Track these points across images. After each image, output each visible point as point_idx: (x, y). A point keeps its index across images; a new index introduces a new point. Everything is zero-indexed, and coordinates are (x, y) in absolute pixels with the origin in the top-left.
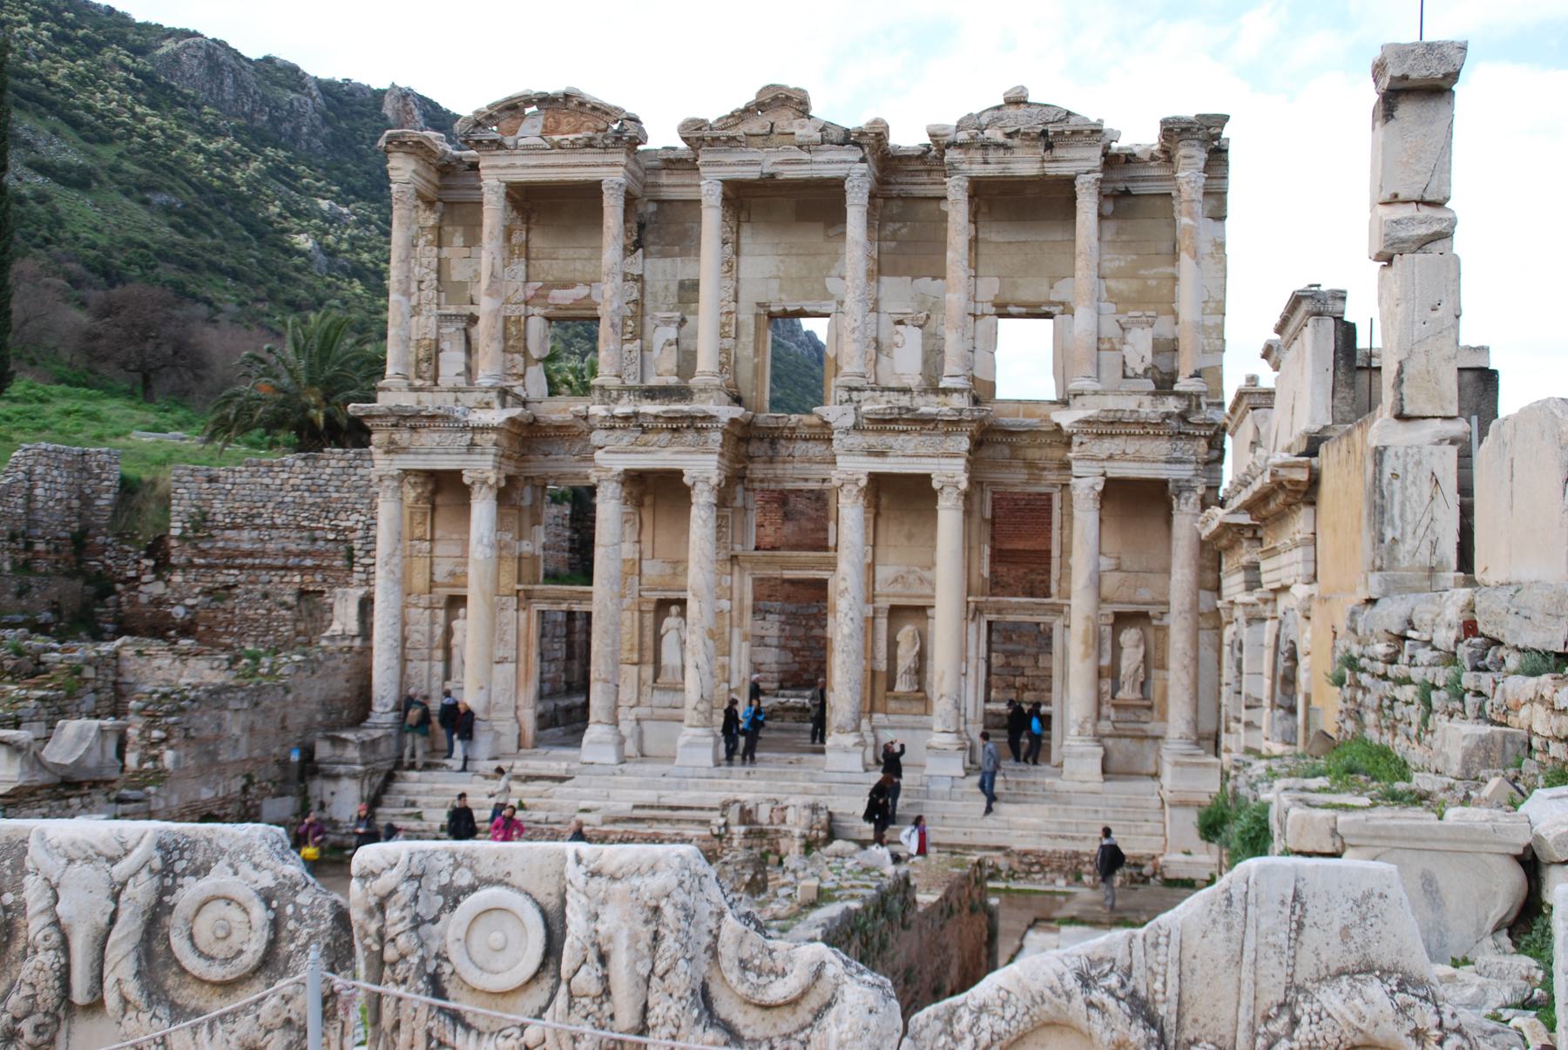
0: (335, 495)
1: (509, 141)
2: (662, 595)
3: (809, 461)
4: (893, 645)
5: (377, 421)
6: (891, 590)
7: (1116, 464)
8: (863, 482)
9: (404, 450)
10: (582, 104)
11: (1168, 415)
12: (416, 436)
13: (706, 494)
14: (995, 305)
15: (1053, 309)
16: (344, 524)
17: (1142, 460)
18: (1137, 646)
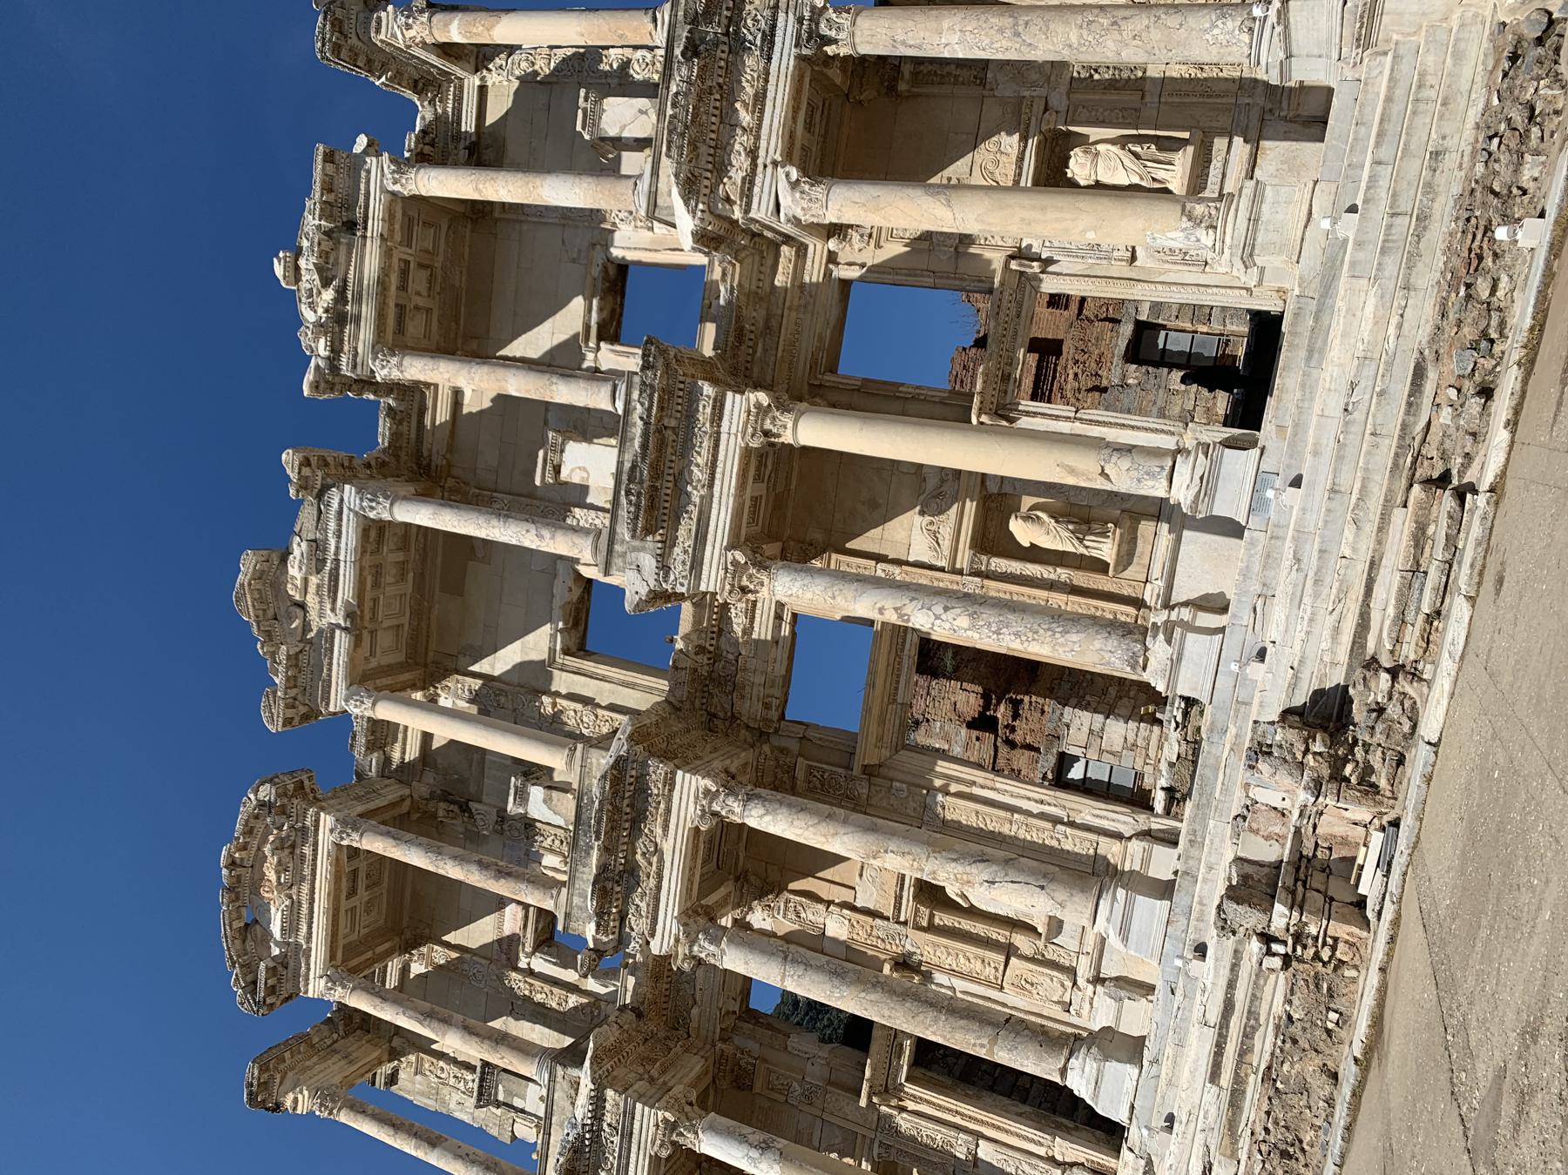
1: (276, 951)
4: (1035, 554)
6: (946, 544)
7: (763, 144)
8: (741, 558)
13: (730, 801)
15: (599, 258)
17: (760, 98)
18: (1097, 154)
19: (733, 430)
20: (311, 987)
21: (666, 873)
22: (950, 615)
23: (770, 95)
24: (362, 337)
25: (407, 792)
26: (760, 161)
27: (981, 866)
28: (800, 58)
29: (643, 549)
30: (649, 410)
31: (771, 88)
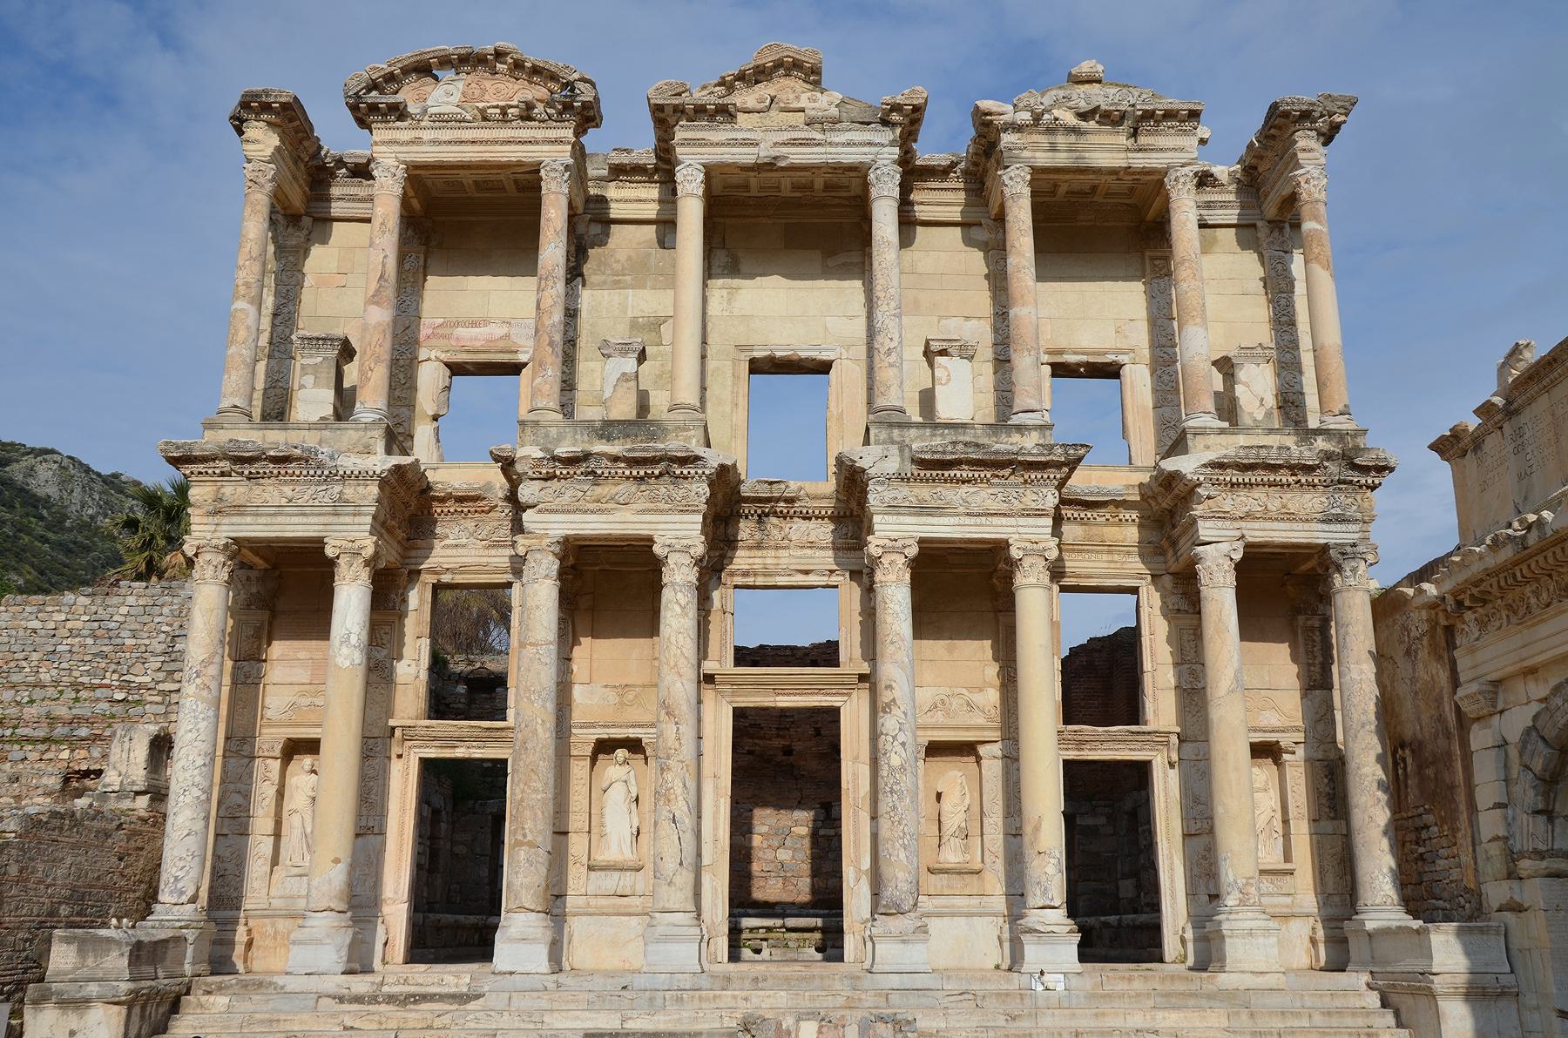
0: (129, 642)
1: (413, 109)
2: (604, 734)
3: (811, 545)
5: (200, 467)
7: (1256, 525)
8: (913, 551)
9: (239, 509)
10: (518, 65)
11: (1328, 456)
12: (257, 490)
13: (685, 570)
14: (1050, 352)
15: (1122, 359)
16: (138, 679)
17: (1291, 517)
19: (1021, 530)
20: (383, 148)
21: (603, 518)
22: (899, 748)
23: (1295, 526)
24: (1038, 154)
25: (580, 211)
26: (1243, 524)
27: (685, 809)
28: (1325, 548)
29: (903, 460)
30: (1030, 454)
31: (1300, 526)
